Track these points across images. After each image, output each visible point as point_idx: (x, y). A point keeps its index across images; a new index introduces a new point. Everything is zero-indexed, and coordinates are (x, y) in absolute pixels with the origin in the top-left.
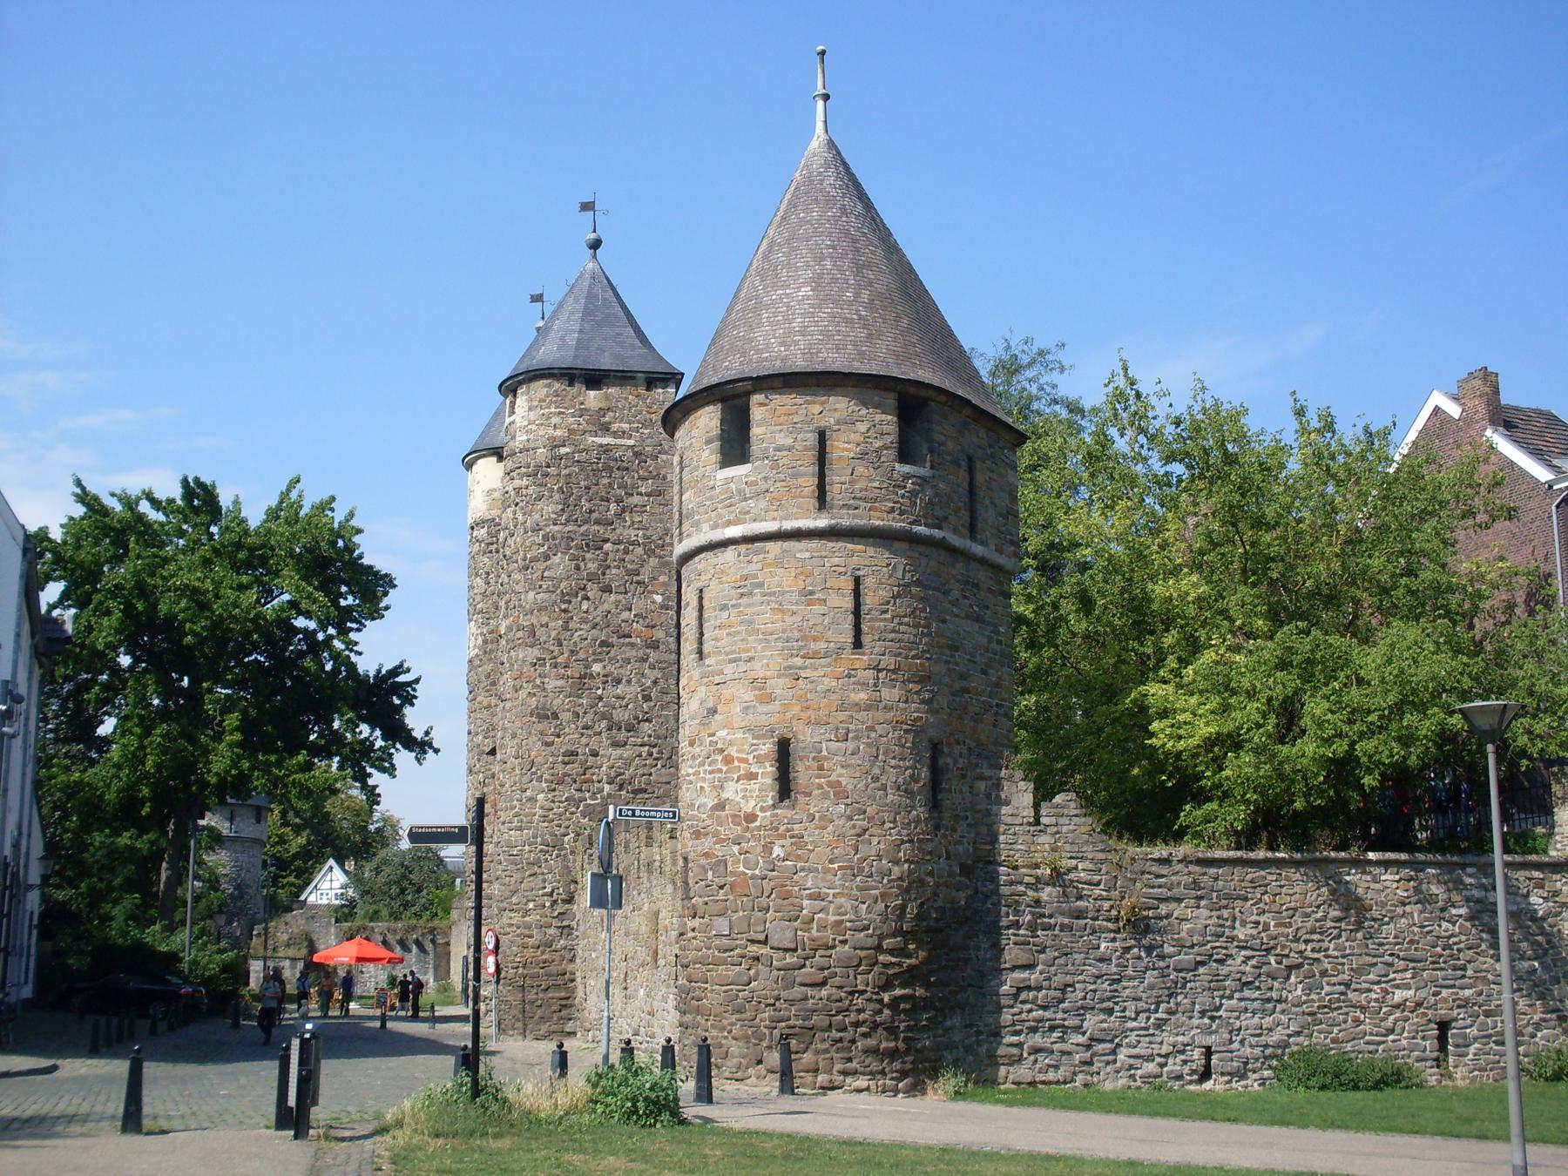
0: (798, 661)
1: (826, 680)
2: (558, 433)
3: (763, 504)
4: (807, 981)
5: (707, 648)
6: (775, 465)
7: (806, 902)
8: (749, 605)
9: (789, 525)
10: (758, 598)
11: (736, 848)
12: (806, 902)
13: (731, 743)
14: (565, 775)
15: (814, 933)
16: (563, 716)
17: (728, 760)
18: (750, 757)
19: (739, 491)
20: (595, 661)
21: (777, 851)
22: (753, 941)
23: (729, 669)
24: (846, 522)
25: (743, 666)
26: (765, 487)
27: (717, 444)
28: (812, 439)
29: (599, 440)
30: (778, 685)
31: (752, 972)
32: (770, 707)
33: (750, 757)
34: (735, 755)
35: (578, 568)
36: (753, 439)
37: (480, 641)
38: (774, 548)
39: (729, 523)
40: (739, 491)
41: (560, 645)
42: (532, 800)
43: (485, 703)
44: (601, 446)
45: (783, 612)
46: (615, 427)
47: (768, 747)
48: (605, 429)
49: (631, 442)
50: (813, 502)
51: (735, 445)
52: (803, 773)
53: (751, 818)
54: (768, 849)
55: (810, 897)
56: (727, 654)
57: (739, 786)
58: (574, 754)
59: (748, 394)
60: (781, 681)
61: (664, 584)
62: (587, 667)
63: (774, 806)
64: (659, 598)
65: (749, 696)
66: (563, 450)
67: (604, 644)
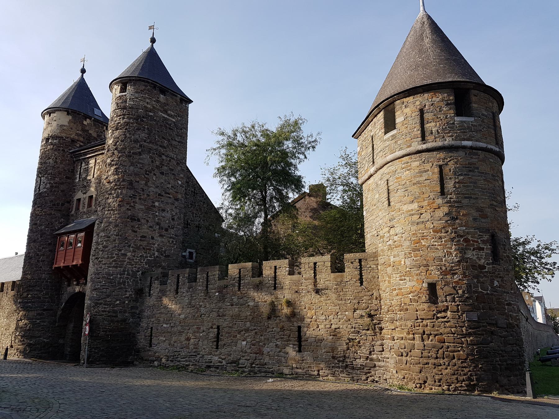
0: (495, 203)
2: (149, 106)
3: (479, 135)
7: (506, 307)
8: (473, 176)
9: (490, 146)
13: (468, 233)
14: (141, 245)
16: (143, 221)
18: (479, 241)
19: (468, 127)
20: (156, 201)
21: (496, 283)
22: (490, 324)
25: (473, 201)
29: (164, 115)
33: (479, 241)
34: (471, 239)
35: (152, 162)
37: (48, 186)
38: (482, 154)
39: (464, 140)
40: (468, 127)
41: (143, 191)
42: (125, 255)
43: (48, 212)
44: (164, 117)
46: (169, 112)
47: (486, 237)
48: (165, 112)
49: (174, 120)
53: (482, 267)
54: (492, 282)
56: (463, 194)
58: (145, 237)
59: (469, 89)
60: (489, 210)
61: (182, 178)
62: (153, 202)
64: (180, 183)
66: (151, 114)
67: (160, 195)
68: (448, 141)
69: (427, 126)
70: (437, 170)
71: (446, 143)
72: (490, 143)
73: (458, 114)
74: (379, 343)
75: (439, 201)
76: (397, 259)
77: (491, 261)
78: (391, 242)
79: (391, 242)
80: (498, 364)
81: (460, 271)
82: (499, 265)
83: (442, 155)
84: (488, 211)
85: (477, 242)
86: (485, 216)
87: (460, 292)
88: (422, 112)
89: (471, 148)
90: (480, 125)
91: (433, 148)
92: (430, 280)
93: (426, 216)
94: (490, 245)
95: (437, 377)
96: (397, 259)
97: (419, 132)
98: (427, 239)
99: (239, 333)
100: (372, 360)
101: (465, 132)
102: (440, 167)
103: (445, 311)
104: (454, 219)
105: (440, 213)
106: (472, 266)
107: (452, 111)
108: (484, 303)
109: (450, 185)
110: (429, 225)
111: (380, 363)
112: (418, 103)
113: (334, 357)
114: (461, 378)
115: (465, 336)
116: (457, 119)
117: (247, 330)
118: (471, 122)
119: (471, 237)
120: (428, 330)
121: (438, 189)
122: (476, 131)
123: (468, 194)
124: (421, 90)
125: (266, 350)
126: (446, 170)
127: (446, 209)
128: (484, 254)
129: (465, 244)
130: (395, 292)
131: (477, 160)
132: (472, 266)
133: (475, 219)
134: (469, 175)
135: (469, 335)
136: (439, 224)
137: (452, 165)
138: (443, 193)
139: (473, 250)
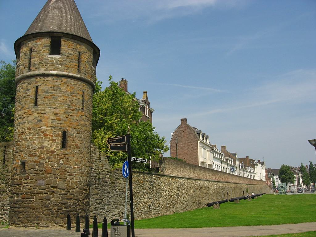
0: (70, 111)
1: (76, 117)
3: (63, 67)
4: (68, 198)
5: (38, 103)
6: (68, 57)
7: (68, 176)
8: (56, 93)
9: (70, 74)
10: (59, 92)
11: (47, 160)
12: (68, 176)
13: (47, 130)
15: (70, 185)
17: (45, 135)
19: (56, 62)
21: (61, 162)
22: (52, 187)
23: (48, 110)
24: (83, 77)
25: (53, 110)
26: (64, 63)
27: (48, 48)
28: (77, 54)
30: (63, 116)
31: (51, 196)
32: (61, 122)
33: (54, 135)
34: (48, 134)
36: (61, 49)
38: (65, 80)
39: (52, 70)
45: (66, 97)
47: (59, 133)
50: (77, 70)
51: (55, 49)
52: (69, 141)
53: (53, 152)
55: (70, 175)
56: (47, 105)
57: (49, 143)
59: (61, 37)
60: (64, 115)
63: (61, 149)
65: (54, 118)
70: (34, 89)
77: (60, 148)
80: (55, 211)
82: (66, 150)
84: (63, 116)
85: (52, 136)
89: (57, 76)
90: (65, 61)
91: (33, 75)
92: (22, 160)
94: (61, 138)
97: (27, 64)
98: (24, 134)
101: (53, 65)
106: (47, 151)
108: (51, 174)
118: (59, 58)
119: (49, 133)
121: (33, 102)
122: (62, 64)
123: (50, 105)
124: (31, 36)
128: (55, 143)
129: (44, 137)
131: (60, 83)
132: (47, 151)
133: (53, 122)
134: (53, 93)
139: (49, 141)
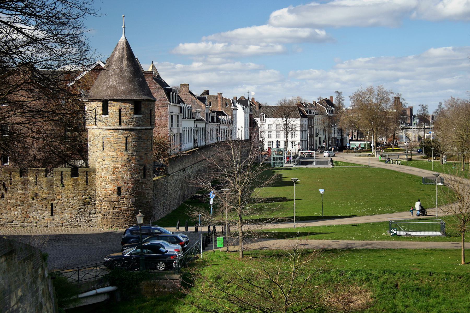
9: (147, 128)
21: (144, 186)
22: (140, 203)
25: (138, 153)
47: (142, 168)
54: (142, 186)
68: (130, 127)
69: (122, 118)
70: (125, 139)
71: (129, 127)
72: (148, 126)
73: (135, 114)
74: (94, 210)
75: (125, 153)
76: (105, 175)
78: (102, 167)
79: (102, 167)
81: (130, 182)
83: (127, 132)
86: (142, 159)
87: (129, 191)
88: (120, 110)
92: (119, 186)
93: (119, 159)
95: (118, 224)
96: (105, 175)
99: (13, 207)
100: (90, 217)
102: (126, 137)
103: (123, 198)
104: (130, 161)
105: (125, 158)
107: (133, 112)
109: (129, 146)
110: (120, 163)
111: (94, 219)
112: (118, 106)
113: (71, 217)
114: (127, 223)
115: (130, 207)
116: (135, 116)
117: (18, 206)
120: (116, 206)
121: (125, 147)
125: (31, 216)
126: (128, 139)
127: (127, 157)
130: (103, 189)
135: (131, 207)
136: (124, 163)
137: (131, 137)
138: (126, 149)
